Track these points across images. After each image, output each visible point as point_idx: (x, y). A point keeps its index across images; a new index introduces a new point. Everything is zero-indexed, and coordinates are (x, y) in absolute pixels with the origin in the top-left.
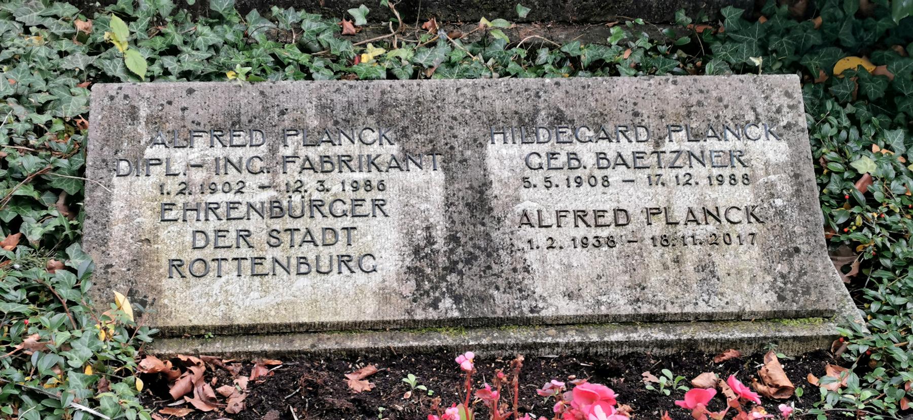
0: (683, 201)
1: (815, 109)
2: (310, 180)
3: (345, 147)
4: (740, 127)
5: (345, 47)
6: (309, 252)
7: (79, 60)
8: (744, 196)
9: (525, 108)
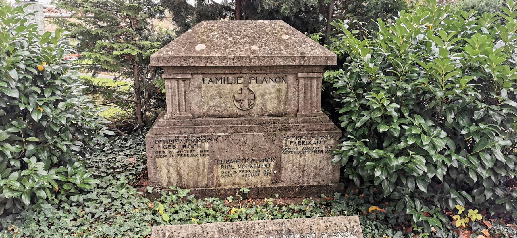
1: (364, 223)
5: (226, 209)
7: (149, 217)
9: (279, 228)
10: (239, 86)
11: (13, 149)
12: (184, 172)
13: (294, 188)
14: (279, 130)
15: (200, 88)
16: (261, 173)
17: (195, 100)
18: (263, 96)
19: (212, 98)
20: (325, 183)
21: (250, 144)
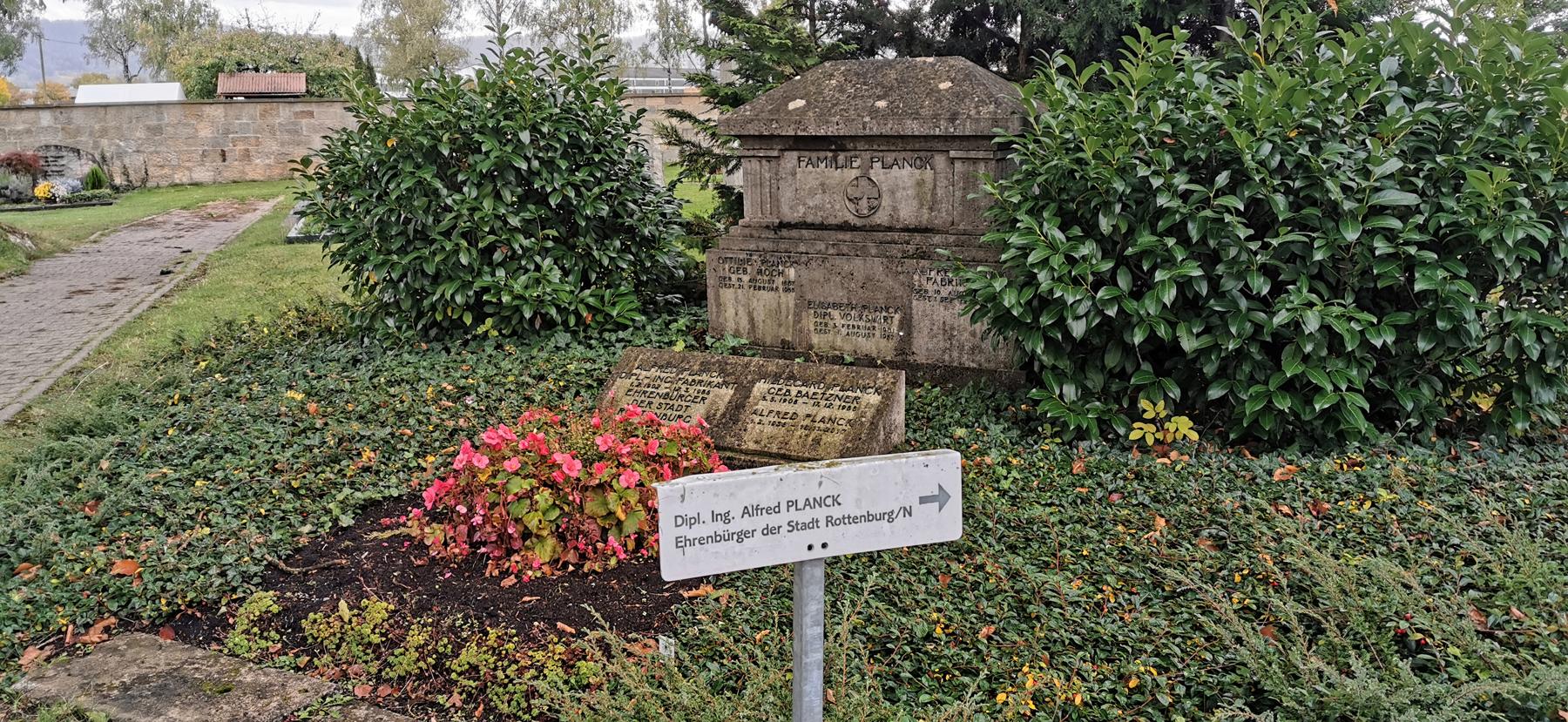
0: (826, 413)
2: (684, 387)
3: (704, 377)
4: (864, 388)
6: (669, 413)
8: (851, 415)
10: (854, 173)
11: (526, 243)
12: (760, 316)
13: (934, 367)
14: (912, 257)
15: (794, 174)
16: (878, 333)
17: (786, 195)
18: (893, 193)
19: (812, 193)
20: (992, 366)
21: (859, 276)
